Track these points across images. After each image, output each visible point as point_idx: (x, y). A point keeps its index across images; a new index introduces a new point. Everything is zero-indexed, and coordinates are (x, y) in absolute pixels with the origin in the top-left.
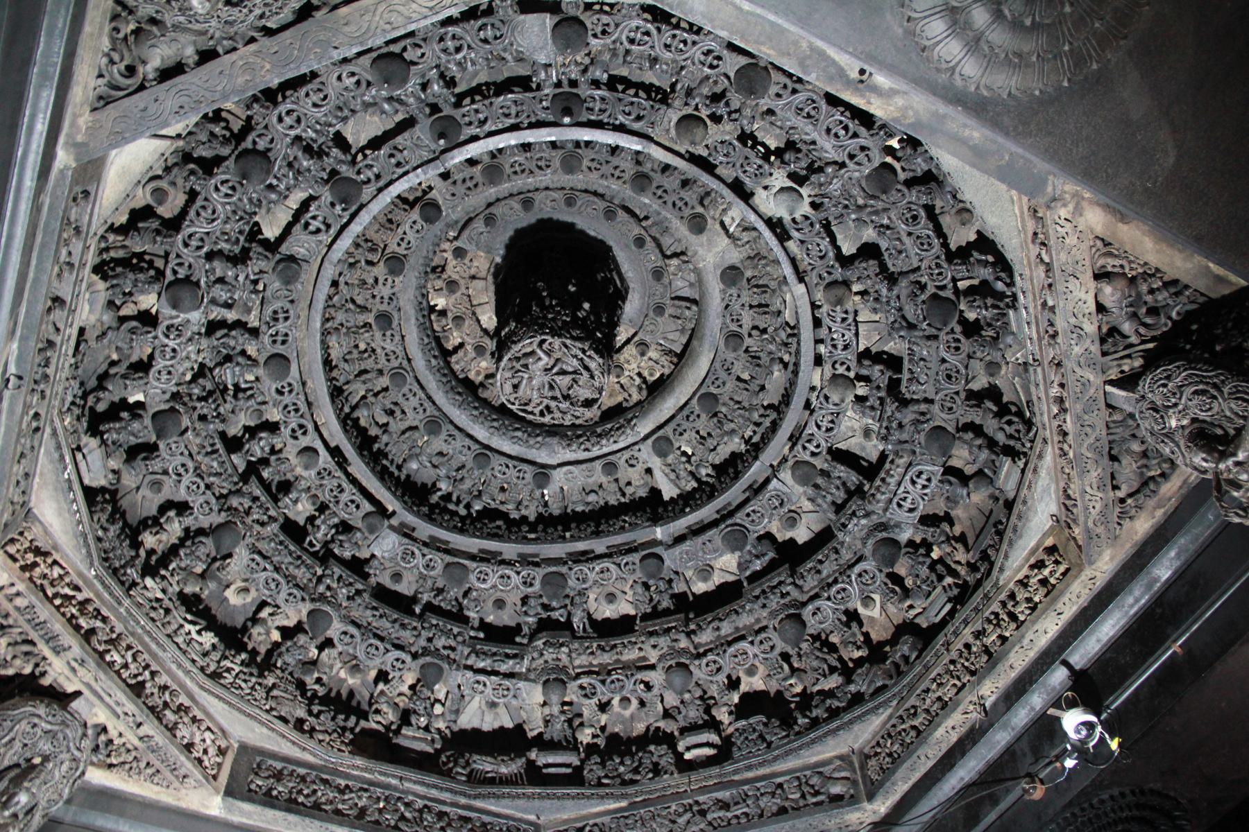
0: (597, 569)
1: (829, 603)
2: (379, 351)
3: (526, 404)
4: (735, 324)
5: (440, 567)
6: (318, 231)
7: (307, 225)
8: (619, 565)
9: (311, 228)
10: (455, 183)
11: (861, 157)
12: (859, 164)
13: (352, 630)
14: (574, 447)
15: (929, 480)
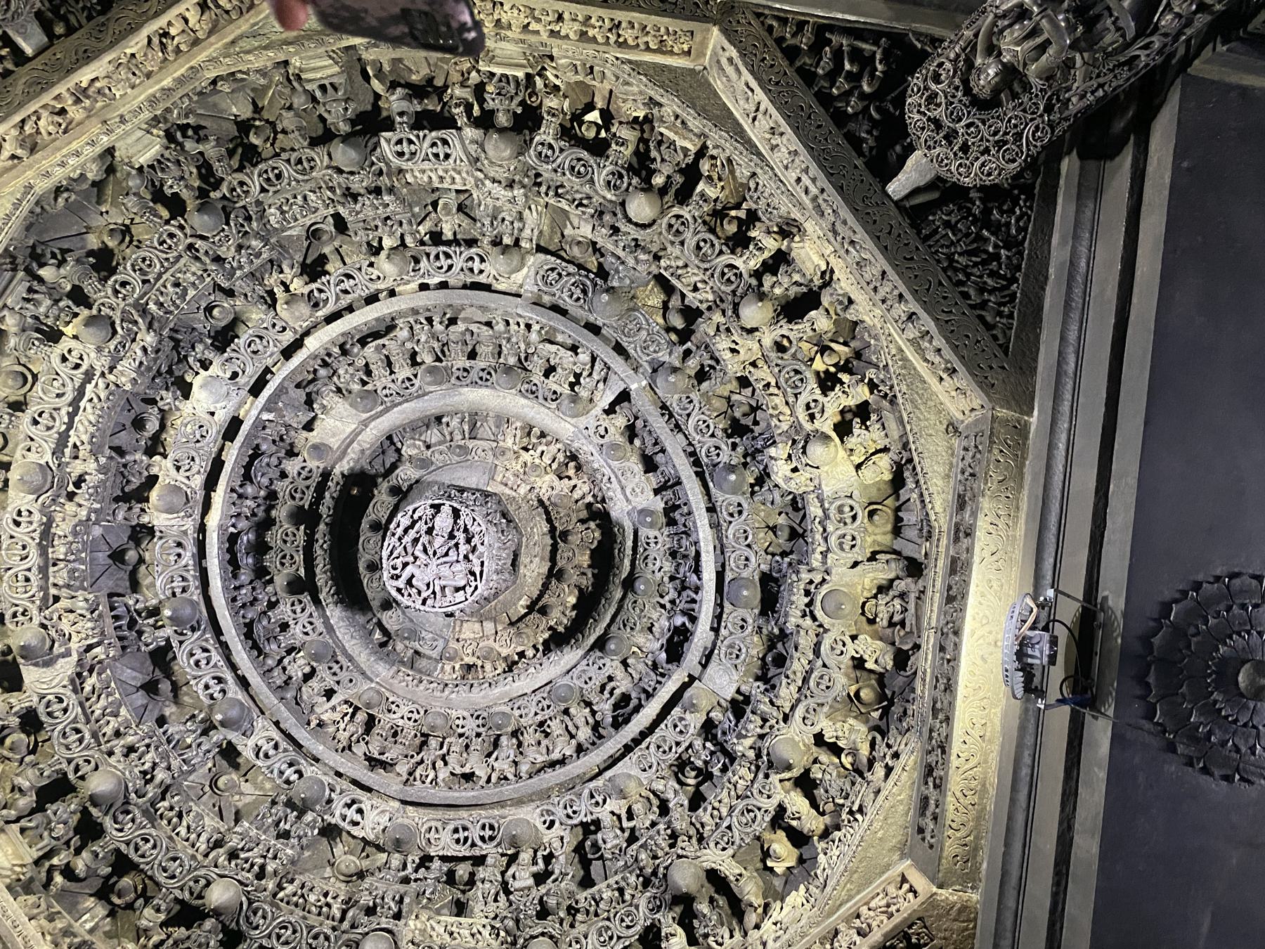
0: (698, 437)
1: (596, 178)
2: (539, 718)
3: (473, 573)
4: (414, 381)
5: (741, 612)
6: (360, 811)
7: (357, 824)
8: (689, 415)
9: (357, 818)
10: (338, 683)
11: (73, 359)
12: (81, 358)
13: (800, 712)
14: (611, 494)
15: (400, 142)
